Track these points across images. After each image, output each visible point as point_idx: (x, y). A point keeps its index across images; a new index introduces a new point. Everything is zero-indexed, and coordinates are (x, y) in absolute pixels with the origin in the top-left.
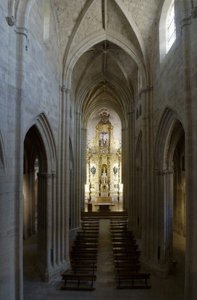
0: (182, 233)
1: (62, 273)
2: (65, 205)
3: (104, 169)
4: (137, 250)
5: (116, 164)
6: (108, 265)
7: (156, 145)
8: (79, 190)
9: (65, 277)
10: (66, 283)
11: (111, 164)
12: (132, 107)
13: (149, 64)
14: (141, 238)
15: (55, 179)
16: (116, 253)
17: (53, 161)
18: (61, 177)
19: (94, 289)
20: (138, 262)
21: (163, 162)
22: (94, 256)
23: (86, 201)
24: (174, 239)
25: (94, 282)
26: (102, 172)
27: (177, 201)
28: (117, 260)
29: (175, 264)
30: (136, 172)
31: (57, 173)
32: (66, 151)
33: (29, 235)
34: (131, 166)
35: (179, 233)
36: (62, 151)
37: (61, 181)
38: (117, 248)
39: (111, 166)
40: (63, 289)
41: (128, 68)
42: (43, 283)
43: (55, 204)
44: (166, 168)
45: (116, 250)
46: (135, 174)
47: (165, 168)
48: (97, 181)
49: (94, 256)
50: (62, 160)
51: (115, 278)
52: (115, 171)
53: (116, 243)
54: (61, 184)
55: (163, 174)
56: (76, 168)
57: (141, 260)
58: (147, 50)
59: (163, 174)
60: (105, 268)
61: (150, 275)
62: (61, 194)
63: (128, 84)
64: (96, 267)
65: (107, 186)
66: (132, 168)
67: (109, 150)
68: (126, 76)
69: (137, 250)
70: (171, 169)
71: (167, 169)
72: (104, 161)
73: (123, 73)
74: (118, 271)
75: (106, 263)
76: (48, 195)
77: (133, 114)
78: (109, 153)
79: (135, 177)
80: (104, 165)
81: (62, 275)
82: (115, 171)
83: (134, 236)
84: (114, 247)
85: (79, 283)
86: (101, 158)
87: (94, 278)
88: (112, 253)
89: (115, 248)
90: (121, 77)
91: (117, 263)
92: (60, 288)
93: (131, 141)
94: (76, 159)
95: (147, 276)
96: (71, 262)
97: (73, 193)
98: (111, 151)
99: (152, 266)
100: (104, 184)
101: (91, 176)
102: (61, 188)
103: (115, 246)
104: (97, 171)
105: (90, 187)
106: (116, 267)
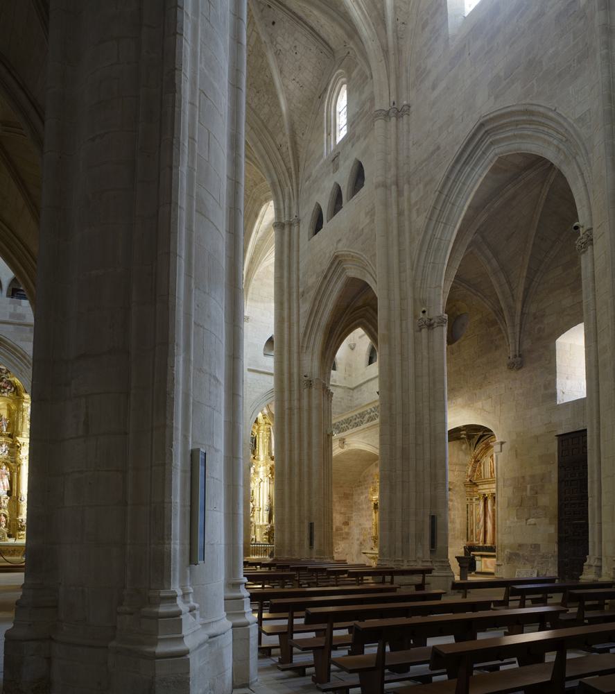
7: (421, 250)
12: (290, 208)
13: (399, 51)
34: (286, 376)
41: (292, 86)
46: (299, 400)
58: (395, 8)
63: (285, 139)
68: (284, 108)
73: (276, 96)
77: (295, 229)
90: (266, 110)
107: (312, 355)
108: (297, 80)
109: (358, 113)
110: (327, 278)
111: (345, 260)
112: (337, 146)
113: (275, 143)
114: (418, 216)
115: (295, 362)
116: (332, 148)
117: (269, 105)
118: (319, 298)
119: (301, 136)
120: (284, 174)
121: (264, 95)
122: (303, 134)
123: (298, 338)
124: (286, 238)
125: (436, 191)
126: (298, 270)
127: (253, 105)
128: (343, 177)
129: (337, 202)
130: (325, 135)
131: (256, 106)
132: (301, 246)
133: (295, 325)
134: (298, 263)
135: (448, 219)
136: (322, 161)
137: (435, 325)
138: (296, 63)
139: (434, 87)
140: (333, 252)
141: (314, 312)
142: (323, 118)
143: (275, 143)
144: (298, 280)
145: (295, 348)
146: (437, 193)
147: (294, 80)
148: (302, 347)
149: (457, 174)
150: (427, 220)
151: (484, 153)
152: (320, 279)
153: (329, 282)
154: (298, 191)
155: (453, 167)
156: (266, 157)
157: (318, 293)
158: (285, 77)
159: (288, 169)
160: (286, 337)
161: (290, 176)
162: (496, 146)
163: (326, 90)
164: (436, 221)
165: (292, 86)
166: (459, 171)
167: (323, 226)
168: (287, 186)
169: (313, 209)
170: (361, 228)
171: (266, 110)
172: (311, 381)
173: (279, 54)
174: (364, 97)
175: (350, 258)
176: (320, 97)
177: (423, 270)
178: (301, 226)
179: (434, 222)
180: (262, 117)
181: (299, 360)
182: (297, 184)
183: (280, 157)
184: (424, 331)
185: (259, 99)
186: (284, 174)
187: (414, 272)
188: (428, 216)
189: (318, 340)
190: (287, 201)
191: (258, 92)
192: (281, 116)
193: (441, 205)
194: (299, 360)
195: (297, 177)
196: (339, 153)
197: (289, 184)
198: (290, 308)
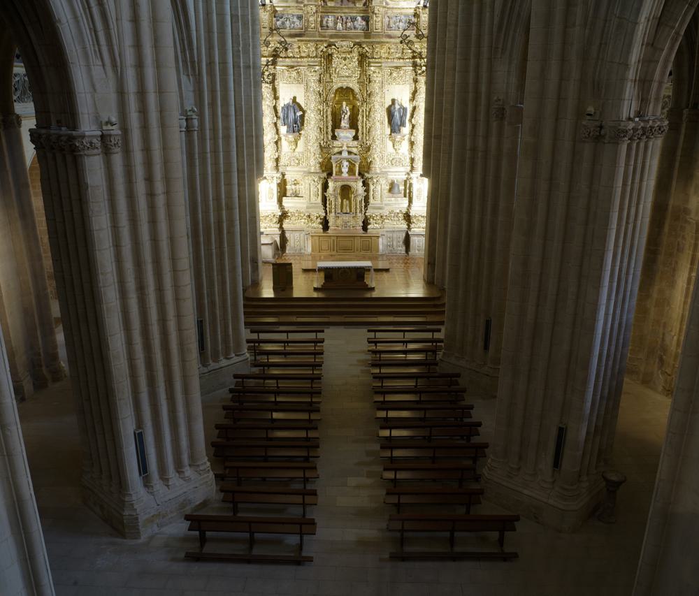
0: (660, 380)
1: (188, 510)
2: (175, 270)
3: (345, 110)
4: (475, 440)
5: (401, 89)
6: (358, 487)
8: (230, 208)
9: (197, 521)
10: (203, 540)
11: (375, 87)
14: (495, 397)
15: (117, 159)
16: (392, 448)
17: (97, 70)
18: (147, 149)
19: (310, 559)
20: (477, 479)
21: (623, 79)
22: (307, 459)
23: (267, 253)
24: (624, 402)
25: (306, 538)
26: (336, 125)
27: (661, 258)
28: (396, 470)
29: (613, 487)
30: (494, 125)
31: (125, 131)
32: (155, 20)
33: (40, 383)
34: (471, 96)
35: (647, 381)
36: (135, 20)
37: (148, 163)
38: (395, 433)
39: (377, 100)
40: (195, 558)
42: (119, 540)
43: (129, 265)
44: (635, 107)
45: (390, 438)
47: (629, 106)
48: (313, 162)
49: (307, 459)
50: (140, 65)
51: (384, 525)
52: (395, 119)
53: (392, 414)
54: (149, 179)
55: (619, 134)
56: (213, 104)
57: (485, 471)
59: (619, 134)
60: (347, 495)
61: (517, 518)
62: (153, 221)
64: (314, 493)
65: (358, 186)
66: (476, 105)
67: (366, 19)
69: (475, 440)
70: (657, 114)
71: (639, 114)
72: (346, 73)
74: (398, 506)
75: (352, 481)
76: (95, 227)
78: (367, 32)
80: (345, 92)
81: (187, 518)
82: (395, 119)
83: (464, 391)
84: (382, 428)
85: (252, 542)
86: (329, 58)
87: (306, 526)
88: (377, 447)
89: (386, 433)
91: (394, 481)
92: (182, 555)
94: (211, 64)
95: (505, 524)
96: (216, 476)
97: (206, 219)
98: (378, 23)
99: (526, 492)
100: (344, 180)
101: (285, 146)
102: (151, 195)
103: (388, 423)
104: (312, 118)
105: (282, 192)
106: (388, 494)
145: (485, 49)
177: (605, 26)
181: (491, 70)
187: (587, 31)
194: (491, 70)
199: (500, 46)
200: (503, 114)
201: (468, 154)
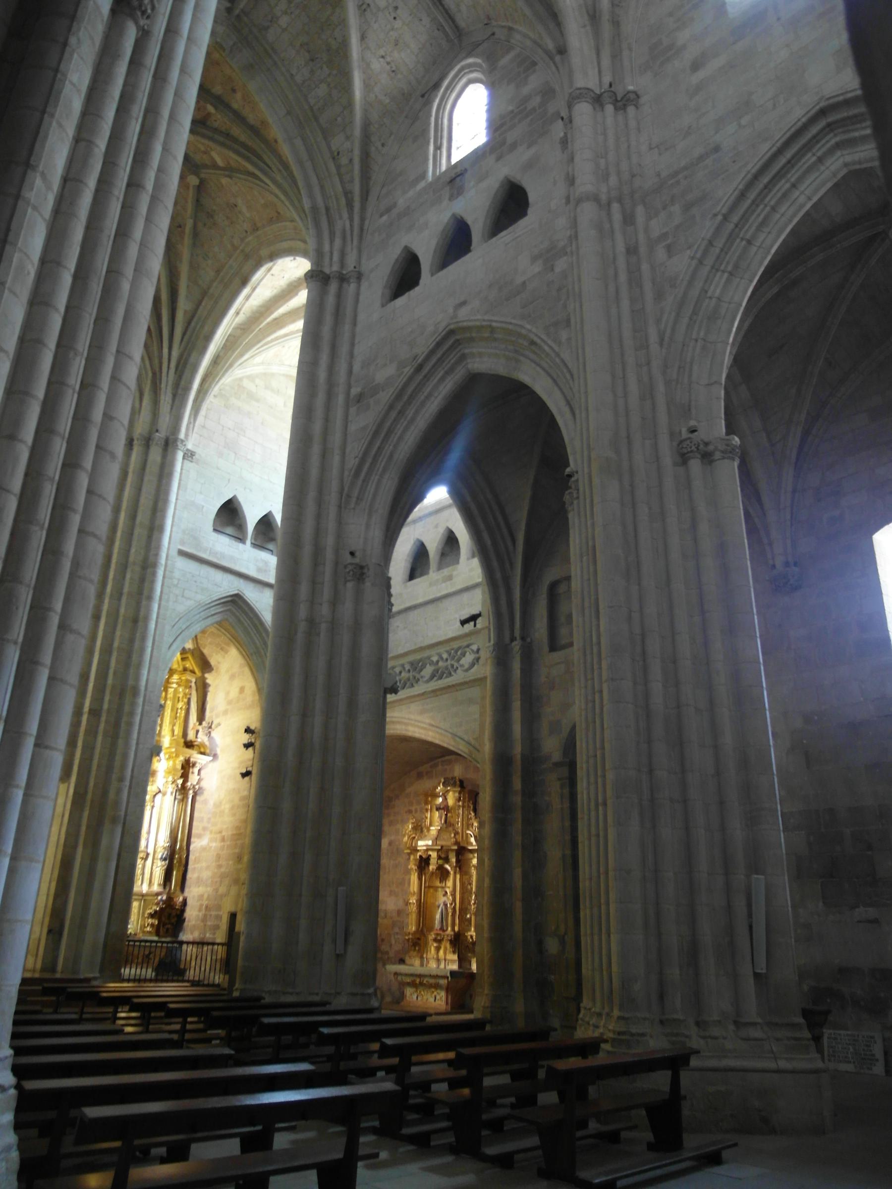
12: (343, 254)
46: (335, 602)
77: (352, 288)
79: (334, 625)
90: (322, 90)
93: (319, 412)
107: (370, 515)
108: (388, 59)
109: (512, 111)
110: (421, 371)
111: (472, 339)
112: (451, 168)
113: (329, 147)
114: (670, 257)
115: (331, 525)
116: (444, 168)
117: (329, 85)
118: (399, 407)
119: (380, 147)
120: (337, 199)
121: (321, 68)
122: (383, 145)
123: (342, 480)
124: (331, 300)
125: (715, 215)
126: (351, 355)
127: (299, 79)
128: (475, 205)
129: (458, 242)
130: (431, 148)
131: (304, 82)
132: (361, 317)
133: (337, 451)
134: (352, 344)
135: (736, 266)
136: (422, 184)
137: (718, 455)
138: (391, 33)
139: (696, 66)
140: (443, 325)
141: (382, 433)
142: (429, 124)
143: (329, 147)
144: (350, 372)
145: (332, 498)
146: (720, 218)
147: (383, 57)
148: (349, 496)
149: (762, 191)
150: (695, 262)
151: (820, 160)
152: (408, 370)
153: (427, 378)
154: (362, 229)
155: (756, 177)
156: (308, 165)
157: (399, 396)
158: (368, 48)
159: (348, 194)
160: (314, 472)
161: (350, 205)
162: (845, 152)
163: (436, 86)
164: (712, 267)
165: (377, 65)
166: (766, 187)
167: (422, 282)
168: (341, 218)
169: (396, 257)
170: (519, 280)
171: (322, 90)
172: (362, 567)
173: (365, 10)
174: (526, 90)
175: (486, 335)
176: (423, 96)
178: (364, 284)
179: (708, 268)
180: (312, 101)
182: (362, 220)
183: (333, 169)
184: (695, 465)
185: (312, 72)
186: (337, 199)
188: (698, 255)
189: (389, 484)
190: (338, 242)
191: (312, 60)
192: (350, 104)
193: (723, 240)
194: (340, 522)
195: (363, 208)
196: (466, 170)
197: (345, 215)
198: (327, 420)
199: (355, 493)
200: (362, 574)
201: (302, 627)
